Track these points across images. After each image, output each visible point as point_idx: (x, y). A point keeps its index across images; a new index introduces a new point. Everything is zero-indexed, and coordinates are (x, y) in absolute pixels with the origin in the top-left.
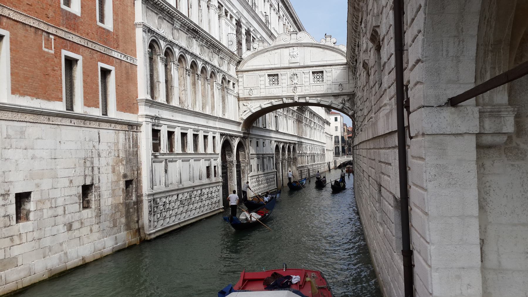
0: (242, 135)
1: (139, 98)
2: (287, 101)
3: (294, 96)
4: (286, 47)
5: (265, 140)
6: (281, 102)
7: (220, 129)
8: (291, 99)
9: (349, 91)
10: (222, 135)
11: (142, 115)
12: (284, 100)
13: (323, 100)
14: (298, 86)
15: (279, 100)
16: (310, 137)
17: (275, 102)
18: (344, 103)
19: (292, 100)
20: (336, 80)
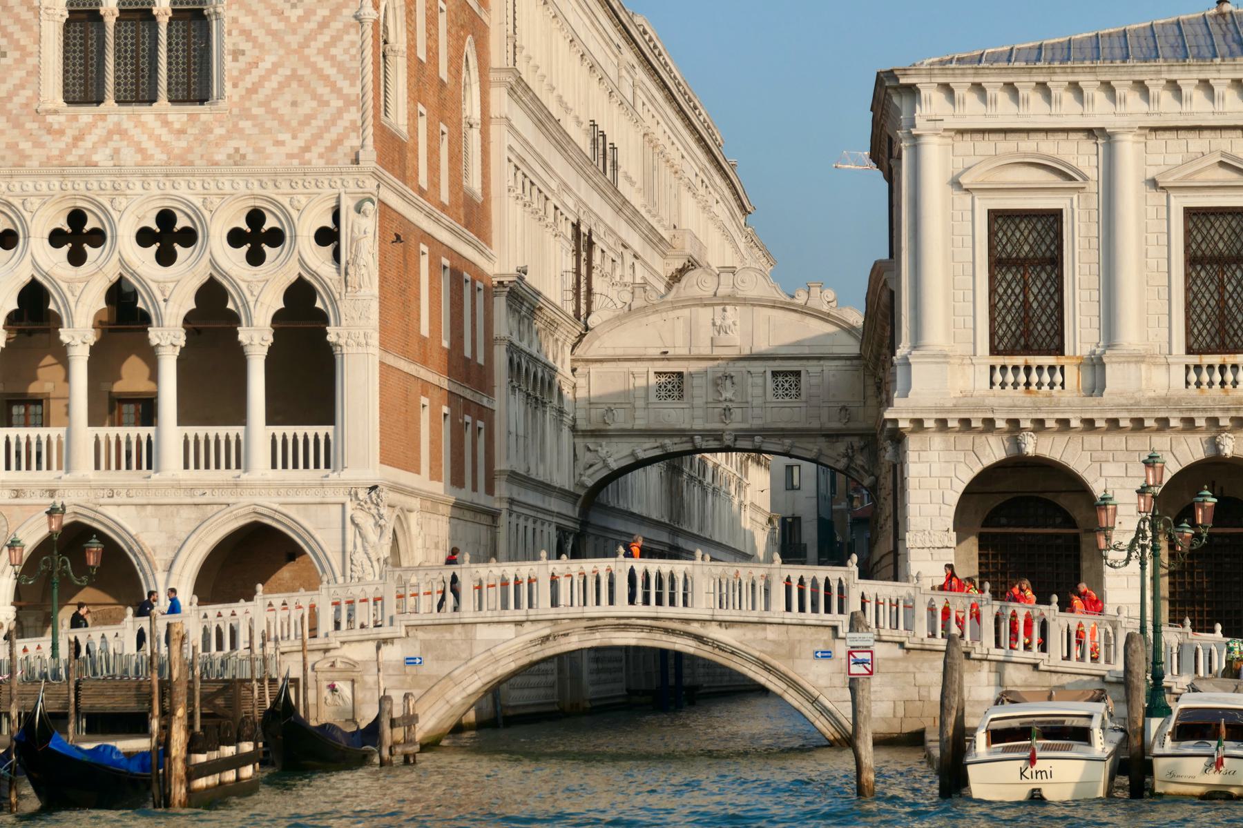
0: (578, 527)
1: (497, 468)
2: (704, 443)
3: (723, 431)
4: (705, 305)
5: (607, 539)
6: (688, 447)
7: (559, 515)
8: (715, 440)
9: (863, 425)
10: (559, 528)
11: (501, 499)
12: (698, 439)
13: (798, 445)
14: (734, 405)
15: (684, 439)
16: (701, 529)
17: (672, 445)
18: (850, 454)
19: (717, 443)
20: (834, 395)
